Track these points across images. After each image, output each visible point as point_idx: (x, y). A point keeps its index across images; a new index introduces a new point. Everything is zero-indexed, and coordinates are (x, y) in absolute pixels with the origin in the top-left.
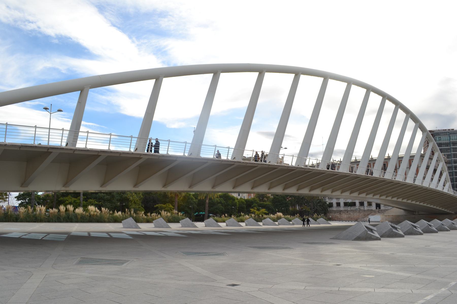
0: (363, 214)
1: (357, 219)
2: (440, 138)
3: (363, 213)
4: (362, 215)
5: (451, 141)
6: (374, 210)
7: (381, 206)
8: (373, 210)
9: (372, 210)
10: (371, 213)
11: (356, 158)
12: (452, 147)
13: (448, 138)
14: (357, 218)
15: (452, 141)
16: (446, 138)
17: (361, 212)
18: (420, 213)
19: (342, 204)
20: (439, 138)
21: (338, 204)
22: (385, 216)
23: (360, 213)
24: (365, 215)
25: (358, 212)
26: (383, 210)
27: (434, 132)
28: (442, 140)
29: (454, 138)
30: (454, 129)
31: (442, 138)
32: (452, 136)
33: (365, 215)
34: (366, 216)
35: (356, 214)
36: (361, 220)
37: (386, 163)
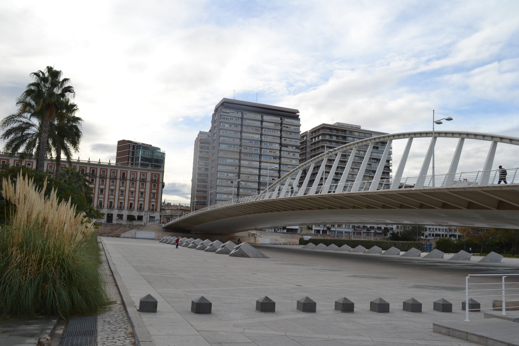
0: (110, 228)
1: (102, 234)
2: (144, 153)
3: (110, 227)
4: (109, 229)
5: (154, 157)
6: (123, 225)
7: (113, 220)
8: (122, 224)
9: (121, 224)
10: (120, 228)
11: (90, 159)
12: (154, 165)
13: (151, 155)
14: (102, 233)
15: (155, 158)
16: (149, 152)
17: (107, 226)
18: (197, 233)
19: (125, 217)
20: (144, 151)
21: (120, 216)
22: (162, 234)
23: (107, 227)
24: (112, 230)
25: (103, 225)
26: (134, 226)
27: (137, 144)
28: (146, 154)
29: (156, 155)
30: (152, 145)
31: (146, 152)
32: (147, 151)
33: (112, 230)
34: (113, 230)
35: (101, 228)
36: (107, 235)
37: (126, 172)
